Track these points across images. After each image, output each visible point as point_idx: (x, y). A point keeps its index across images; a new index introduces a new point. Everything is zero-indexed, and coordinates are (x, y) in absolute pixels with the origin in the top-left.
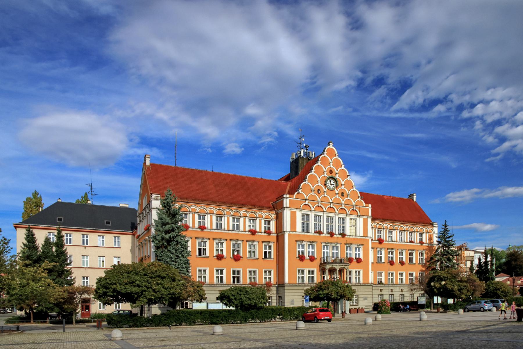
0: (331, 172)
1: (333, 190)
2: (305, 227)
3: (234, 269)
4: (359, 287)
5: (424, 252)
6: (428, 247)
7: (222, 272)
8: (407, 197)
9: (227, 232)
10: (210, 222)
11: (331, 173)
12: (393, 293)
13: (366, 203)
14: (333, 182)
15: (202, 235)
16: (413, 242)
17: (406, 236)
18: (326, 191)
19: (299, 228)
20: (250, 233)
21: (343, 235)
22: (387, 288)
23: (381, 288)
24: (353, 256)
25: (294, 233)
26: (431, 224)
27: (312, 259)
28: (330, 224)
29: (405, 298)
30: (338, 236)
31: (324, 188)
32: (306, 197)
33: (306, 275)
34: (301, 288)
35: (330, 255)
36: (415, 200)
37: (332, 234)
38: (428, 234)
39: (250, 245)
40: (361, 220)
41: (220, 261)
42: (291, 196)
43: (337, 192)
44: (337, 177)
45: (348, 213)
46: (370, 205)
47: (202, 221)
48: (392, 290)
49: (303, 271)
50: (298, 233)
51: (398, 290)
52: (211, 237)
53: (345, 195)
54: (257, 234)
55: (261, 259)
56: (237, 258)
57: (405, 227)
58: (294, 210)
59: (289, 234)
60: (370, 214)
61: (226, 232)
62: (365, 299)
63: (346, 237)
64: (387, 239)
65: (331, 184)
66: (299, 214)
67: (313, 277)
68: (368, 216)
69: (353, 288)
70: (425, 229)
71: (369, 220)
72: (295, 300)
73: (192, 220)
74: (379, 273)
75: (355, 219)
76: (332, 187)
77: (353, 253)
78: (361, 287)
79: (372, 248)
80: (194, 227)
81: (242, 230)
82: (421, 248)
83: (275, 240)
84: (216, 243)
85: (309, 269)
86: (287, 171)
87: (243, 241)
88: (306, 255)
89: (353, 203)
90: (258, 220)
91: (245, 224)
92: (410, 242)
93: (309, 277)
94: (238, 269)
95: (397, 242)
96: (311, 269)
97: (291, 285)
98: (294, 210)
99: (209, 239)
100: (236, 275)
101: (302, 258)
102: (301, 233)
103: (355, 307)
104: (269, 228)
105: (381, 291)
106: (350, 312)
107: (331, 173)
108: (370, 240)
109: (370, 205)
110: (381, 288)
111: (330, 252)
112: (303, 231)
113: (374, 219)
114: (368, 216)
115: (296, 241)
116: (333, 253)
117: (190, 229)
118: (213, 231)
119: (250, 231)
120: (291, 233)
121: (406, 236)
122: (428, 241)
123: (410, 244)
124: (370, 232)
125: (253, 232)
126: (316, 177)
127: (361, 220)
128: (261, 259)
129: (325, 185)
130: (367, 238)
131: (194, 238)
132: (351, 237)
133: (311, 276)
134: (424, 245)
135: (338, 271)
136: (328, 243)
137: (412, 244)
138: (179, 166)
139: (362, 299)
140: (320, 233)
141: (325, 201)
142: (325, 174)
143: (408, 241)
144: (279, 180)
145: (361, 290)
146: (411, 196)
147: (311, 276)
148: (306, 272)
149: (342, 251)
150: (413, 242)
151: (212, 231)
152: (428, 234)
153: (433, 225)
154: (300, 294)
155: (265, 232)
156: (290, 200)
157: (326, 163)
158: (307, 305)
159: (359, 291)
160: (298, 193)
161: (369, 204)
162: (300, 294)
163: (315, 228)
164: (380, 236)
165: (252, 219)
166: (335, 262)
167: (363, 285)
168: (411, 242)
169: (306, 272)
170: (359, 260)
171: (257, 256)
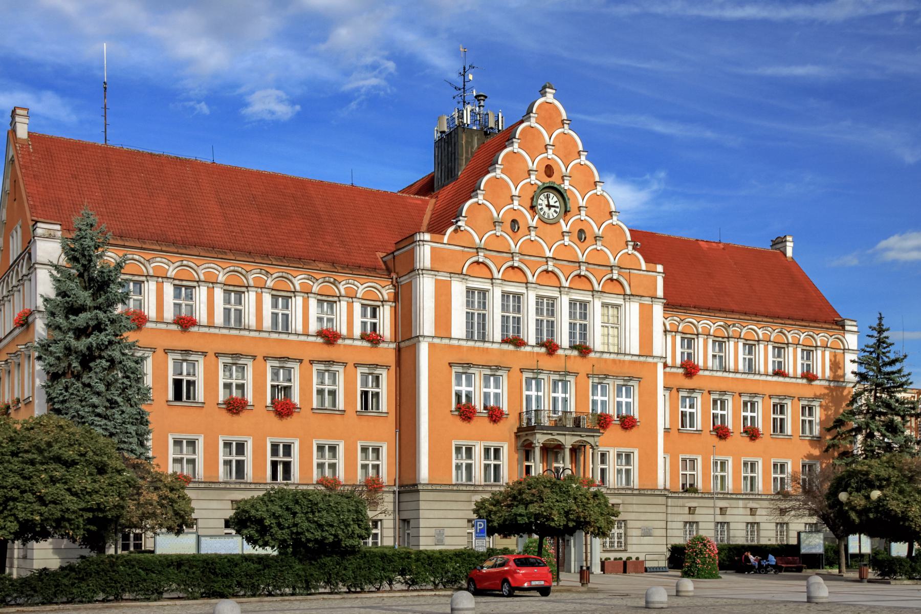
0: (549, 170)
1: (555, 222)
2: (477, 326)
3: (276, 440)
4: (629, 499)
5: (816, 403)
6: (828, 388)
7: (241, 448)
8: (767, 246)
9: (256, 334)
10: (208, 304)
13: (647, 261)
14: (554, 199)
15: (184, 341)
16: (784, 375)
17: (765, 358)
18: (534, 224)
19: (458, 328)
20: (320, 340)
21: (584, 350)
22: (710, 503)
23: (693, 504)
24: (612, 411)
25: (446, 341)
26: (836, 323)
27: (495, 415)
29: (762, 533)
30: (569, 352)
31: (529, 217)
32: (477, 240)
33: (478, 461)
34: (463, 496)
35: (546, 405)
36: (789, 253)
37: (551, 348)
38: (827, 353)
39: (321, 374)
40: (633, 309)
41: (236, 418)
42: (437, 237)
43: (565, 229)
44: (566, 185)
45: (596, 287)
46: (660, 268)
47: (183, 303)
48: (723, 511)
49: (469, 450)
50: (455, 342)
51: (741, 511)
52: (211, 348)
53: (590, 239)
54: (340, 341)
55: (350, 413)
56: (283, 409)
57: (760, 332)
58: (443, 277)
59: (431, 346)
60: (660, 293)
61: (253, 334)
62: (647, 533)
63: (592, 355)
64: (710, 364)
65: (549, 206)
66: (458, 289)
67: (497, 467)
68: (654, 298)
69: (612, 500)
70: (821, 337)
71: (658, 310)
72: (447, 532)
73: (155, 300)
74: (684, 460)
75: (617, 306)
76: (552, 213)
77: (610, 401)
78: (635, 499)
79: (666, 388)
80: (160, 320)
81: (300, 329)
82: (809, 392)
83: (391, 359)
84: (225, 365)
85: (488, 444)
86: (424, 166)
87: (301, 361)
88: (478, 404)
89: (612, 261)
90: (344, 304)
91: (305, 315)
92: (776, 374)
93: (487, 467)
94: (287, 440)
95: (736, 372)
96: (493, 444)
97: (433, 487)
98: (443, 277)
99: (204, 354)
100: (281, 458)
101: (466, 412)
102: (463, 343)
103: (618, 555)
104: (374, 325)
105: (692, 511)
106: (603, 569)
107: (550, 176)
108: (660, 366)
109: (660, 268)
110: (693, 504)
111: (549, 398)
112: (470, 337)
113: (670, 306)
114: (654, 298)
115: (450, 365)
116: (555, 400)
117: (148, 325)
118: (216, 331)
119: (320, 334)
120: (436, 341)
121: (765, 358)
122: (828, 373)
123: (775, 379)
124: (659, 344)
125: (330, 337)
126: (506, 186)
127: (633, 309)
128: (350, 413)
129: (532, 207)
130: (650, 360)
131: (160, 352)
132: (606, 356)
133: (492, 462)
134: (816, 383)
135: (567, 452)
136: (540, 371)
137: (781, 379)
139: (639, 532)
140: (518, 342)
141: (531, 253)
142: (533, 177)
143: (770, 371)
144: (403, 191)
145: (635, 508)
146: (779, 242)
147: (492, 462)
148: (478, 452)
149: (581, 396)
150: (784, 375)
151: (212, 330)
152: (827, 353)
153: (843, 326)
154: (461, 514)
155: (364, 337)
156: (432, 248)
157: (534, 145)
158: (482, 545)
159: (630, 508)
160: (456, 231)
161: (656, 263)
162: (461, 514)
163: (505, 328)
164: (689, 355)
165: (328, 301)
166: (559, 426)
167: (641, 492)
168: (779, 373)
169: (478, 452)
170: (627, 423)
171: (341, 405)
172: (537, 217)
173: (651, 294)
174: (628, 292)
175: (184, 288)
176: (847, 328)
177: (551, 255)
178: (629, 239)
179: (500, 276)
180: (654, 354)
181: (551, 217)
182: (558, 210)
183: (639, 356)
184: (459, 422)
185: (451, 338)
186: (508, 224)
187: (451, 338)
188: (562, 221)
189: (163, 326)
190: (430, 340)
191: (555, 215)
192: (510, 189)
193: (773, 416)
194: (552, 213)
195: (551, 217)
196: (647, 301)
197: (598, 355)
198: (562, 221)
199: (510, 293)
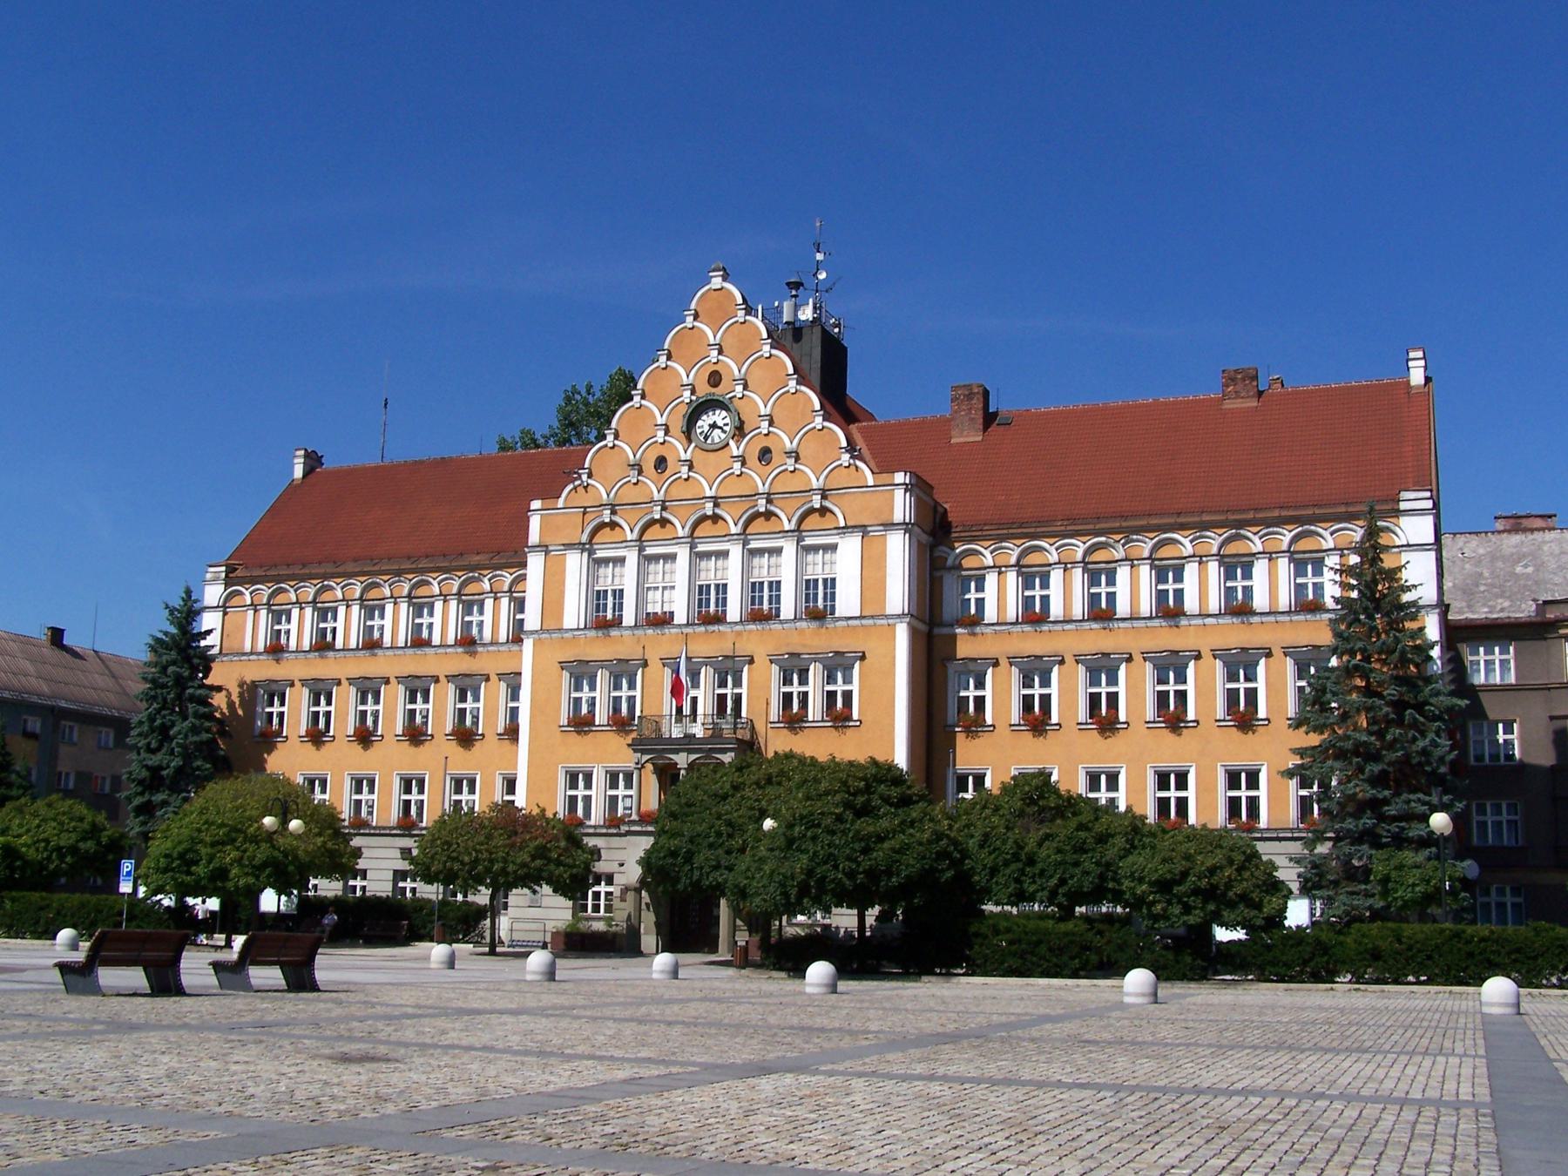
11: (715, 385)
14: (719, 417)
43: (735, 453)
46: (900, 477)
53: (777, 457)
69: (591, 842)
114: (890, 526)
121: (1201, 587)
148: (599, 778)
169: (599, 778)
173: (883, 519)
175: (1032, 576)
180: (888, 612)
183: (862, 617)
184: (358, 748)
186: (649, 466)
188: (732, 443)
193: (285, 709)
198: (732, 443)
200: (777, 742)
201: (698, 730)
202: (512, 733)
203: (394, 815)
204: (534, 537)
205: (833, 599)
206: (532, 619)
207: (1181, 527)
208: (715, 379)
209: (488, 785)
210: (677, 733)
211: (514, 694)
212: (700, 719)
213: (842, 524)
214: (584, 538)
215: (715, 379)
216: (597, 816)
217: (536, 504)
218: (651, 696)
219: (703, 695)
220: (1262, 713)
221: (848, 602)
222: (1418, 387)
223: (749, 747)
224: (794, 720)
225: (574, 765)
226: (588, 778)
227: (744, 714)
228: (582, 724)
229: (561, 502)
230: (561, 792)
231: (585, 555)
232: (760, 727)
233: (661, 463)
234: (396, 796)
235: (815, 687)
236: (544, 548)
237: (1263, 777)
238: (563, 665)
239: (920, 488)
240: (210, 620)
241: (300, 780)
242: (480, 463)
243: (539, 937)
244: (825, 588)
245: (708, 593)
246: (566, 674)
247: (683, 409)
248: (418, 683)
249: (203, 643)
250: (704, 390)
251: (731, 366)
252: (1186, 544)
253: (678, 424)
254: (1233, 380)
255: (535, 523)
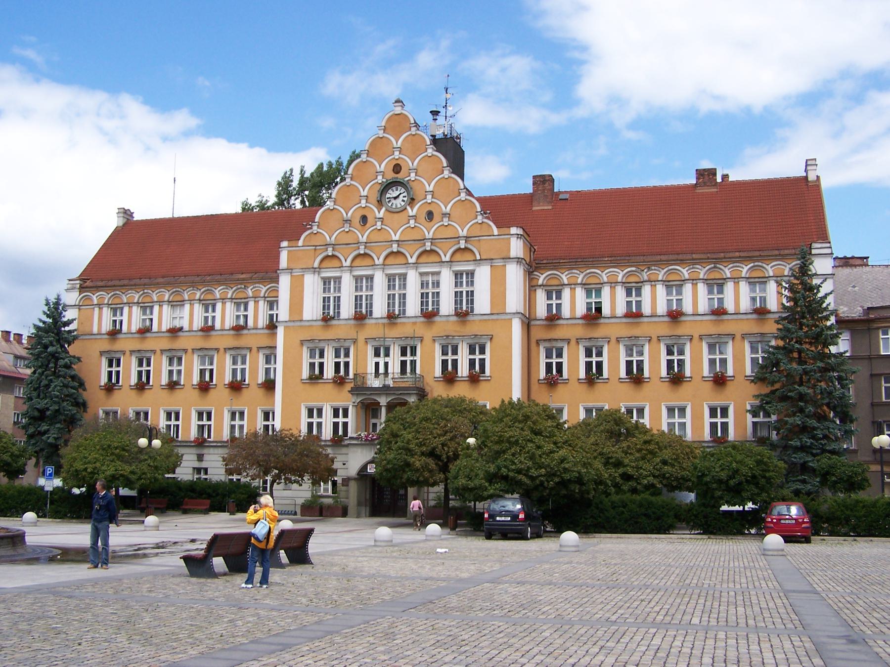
11: (398, 173)
12: (204, 465)
18: (381, 215)
25: (298, 324)
28: (364, 294)
33: (328, 420)
42: (293, 243)
46: (514, 230)
53: (437, 216)
59: (286, 327)
76: (399, 203)
89: (461, 234)
130: (503, 317)
135: (384, 410)
138: (176, 216)
165: (716, 285)
169: (328, 412)
172: (384, 209)
174: (478, 258)
176: (813, 252)
177: (397, 238)
178: (479, 209)
179: (348, 263)
181: (399, 206)
182: (405, 199)
185: (301, 321)
186: (357, 221)
187: (301, 321)
188: (408, 208)
189: (130, 336)
190: (285, 324)
191: (403, 204)
192: (359, 191)
194: (399, 203)
195: (399, 206)
196: (499, 263)
197: (444, 319)
198: (408, 208)
199: (394, 275)
200: (438, 391)
201: (390, 382)
202: (269, 385)
203: (193, 434)
204: (284, 261)
205: (472, 303)
206: (283, 312)
207: (681, 262)
208: (397, 168)
209: (253, 417)
210: (376, 383)
211: (269, 359)
212: (390, 376)
213: (478, 258)
214: (316, 265)
215: (397, 168)
216: (327, 433)
217: (285, 244)
218: (365, 364)
219: (394, 361)
220: (646, 374)
221: (482, 304)
222: (812, 182)
223: (422, 394)
224: (449, 377)
225: (311, 404)
226: (320, 412)
227: (418, 371)
228: (316, 377)
229: (300, 243)
230: (304, 420)
231: (317, 275)
232: (429, 380)
233: (364, 219)
234: (194, 422)
235: (463, 358)
236: (289, 270)
237: (647, 412)
238: (302, 342)
239: (528, 237)
240: (69, 315)
241: (623, 410)
242: (236, 216)
243: (291, 508)
244: (467, 296)
245: (329, 301)
246: (305, 349)
247: (378, 187)
248: (174, 353)
249: (67, 329)
250: (391, 176)
251: (408, 162)
252: (685, 273)
253: (375, 196)
254: (702, 175)
255: (284, 257)
